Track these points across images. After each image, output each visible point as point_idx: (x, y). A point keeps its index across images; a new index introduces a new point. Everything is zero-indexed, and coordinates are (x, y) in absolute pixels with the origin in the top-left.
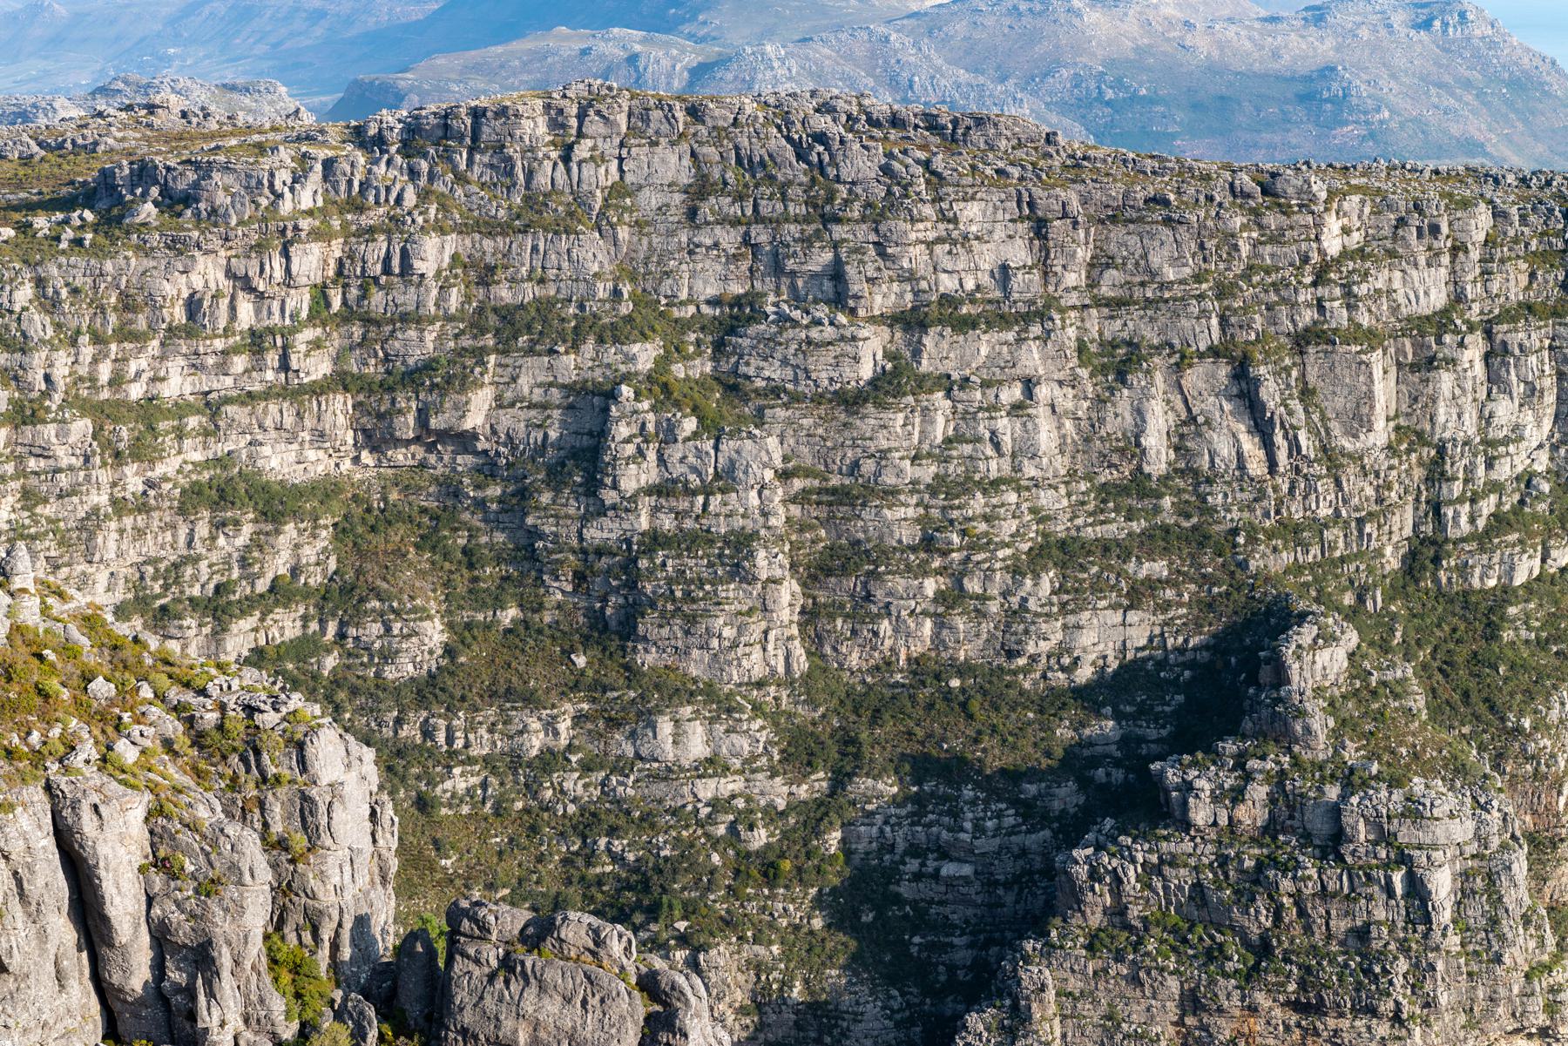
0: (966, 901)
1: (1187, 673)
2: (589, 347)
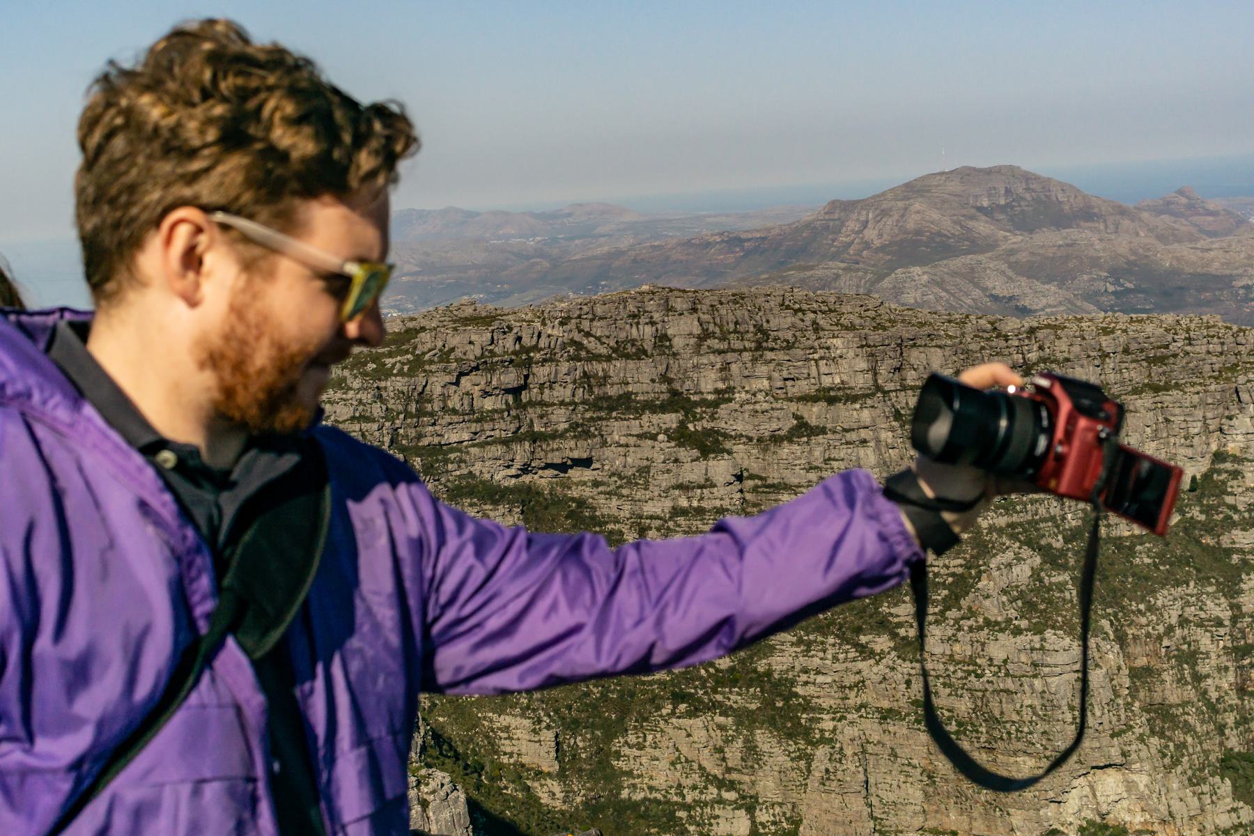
1: (950, 579)
2: (645, 418)
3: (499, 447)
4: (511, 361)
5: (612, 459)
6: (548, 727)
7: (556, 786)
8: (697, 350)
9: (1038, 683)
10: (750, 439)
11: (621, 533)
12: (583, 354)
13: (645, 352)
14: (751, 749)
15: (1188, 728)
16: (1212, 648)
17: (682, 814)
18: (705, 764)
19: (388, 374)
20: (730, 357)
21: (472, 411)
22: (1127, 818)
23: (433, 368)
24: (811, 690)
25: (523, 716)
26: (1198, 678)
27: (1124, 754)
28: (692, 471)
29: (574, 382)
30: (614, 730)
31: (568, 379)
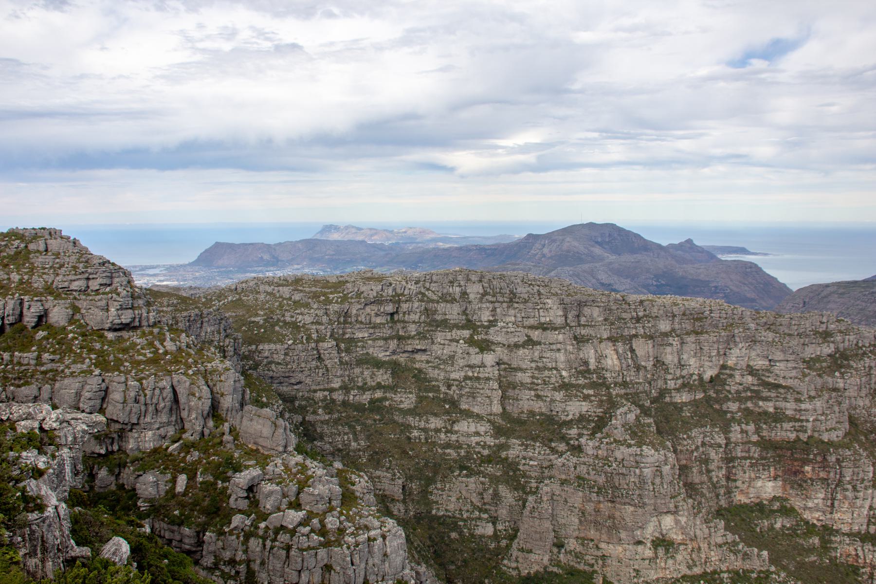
0: (535, 471)
2: (454, 331)
5: (437, 350)
6: (399, 478)
7: (401, 507)
8: (481, 301)
9: (637, 471)
10: (504, 345)
11: (439, 387)
13: (455, 300)
14: (496, 495)
15: (703, 495)
16: (716, 457)
17: (461, 523)
18: (473, 500)
19: (331, 302)
20: (497, 305)
21: (370, 323)
22: (675, 537)
23: (353, 301)
24: (527, 467)
25: (387, 471)
26: (709, 471)
27: (676, 507)
28: (476, 358)
30: (430, 481)
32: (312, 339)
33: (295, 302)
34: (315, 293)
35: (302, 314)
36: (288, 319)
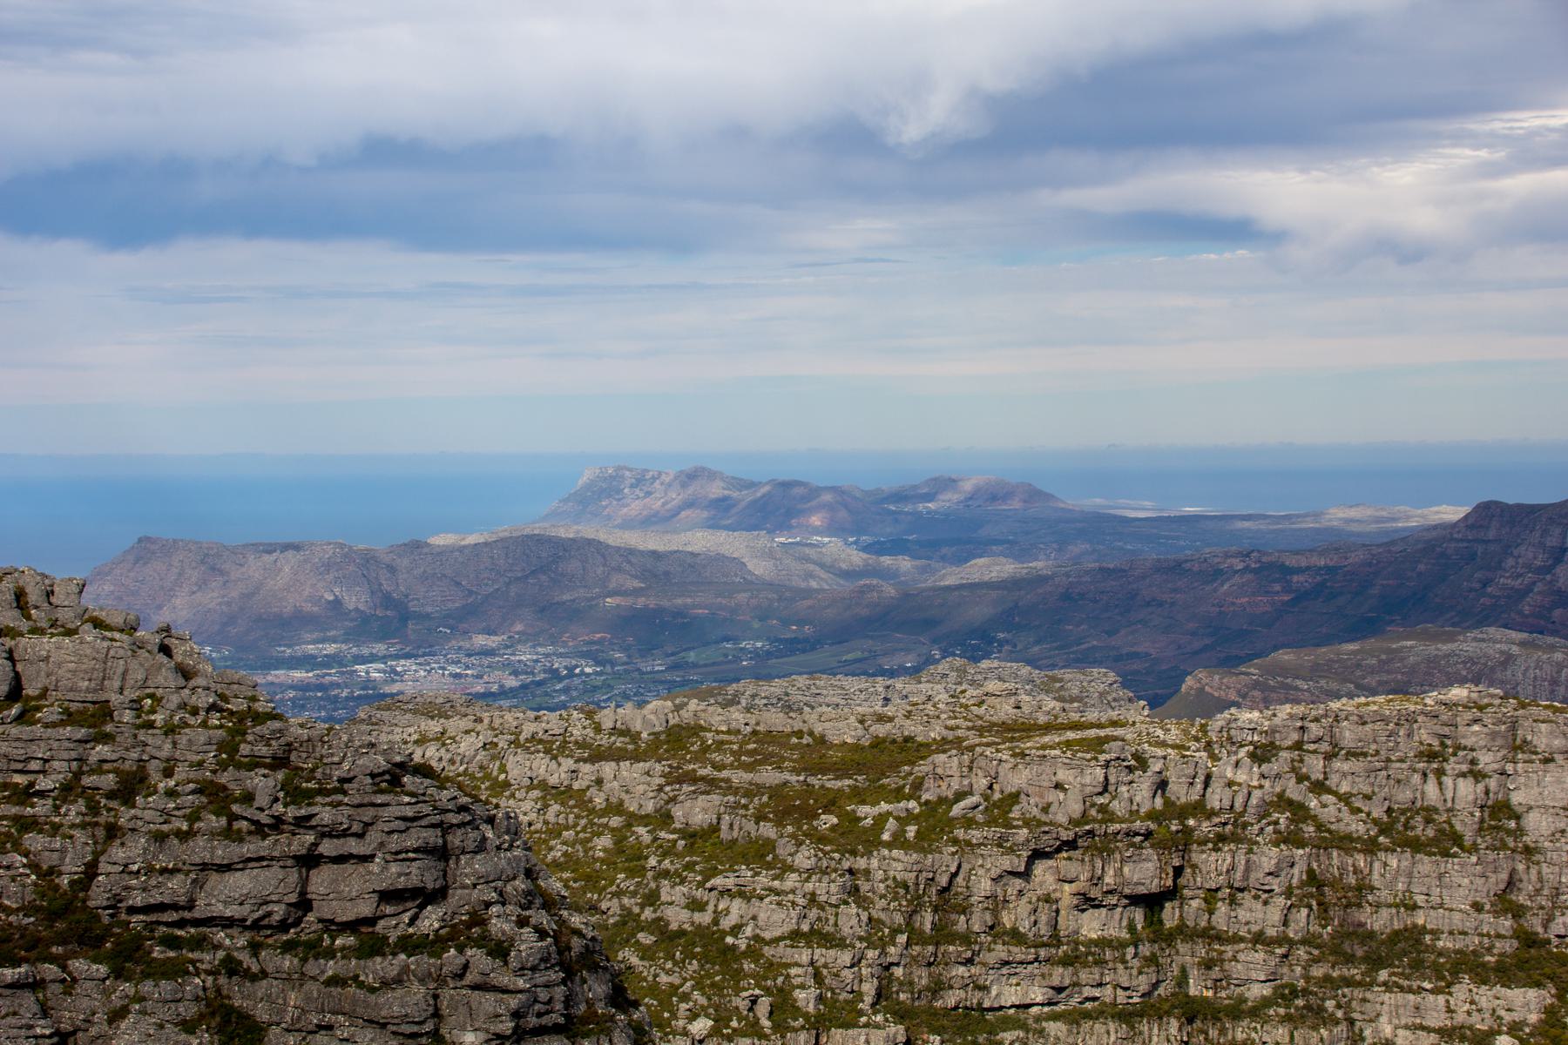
2: (1461, 991)
3: (1112, 1026)
4: (1148, 835)
12: (1309, 829)
13: (1457, 839)
19: (871, 841)
21: (1055, 939)
23: (975, 835)
29: (1288, 893)
31: (1276, 885)
32: (797, 1011)
33: (692, 836)
34: (776, 792)
35: (742, 894)
36: (678, 917)
